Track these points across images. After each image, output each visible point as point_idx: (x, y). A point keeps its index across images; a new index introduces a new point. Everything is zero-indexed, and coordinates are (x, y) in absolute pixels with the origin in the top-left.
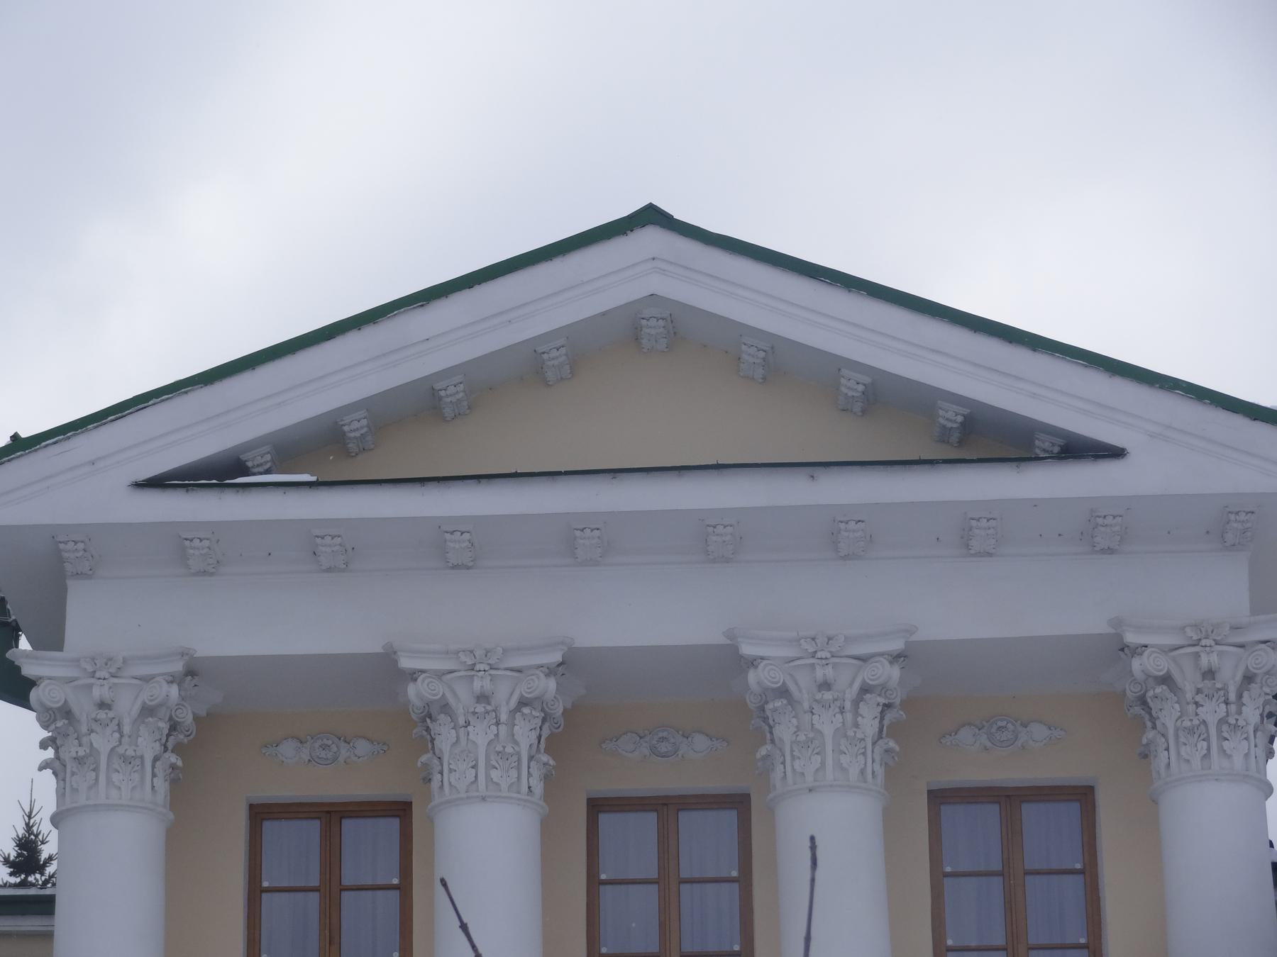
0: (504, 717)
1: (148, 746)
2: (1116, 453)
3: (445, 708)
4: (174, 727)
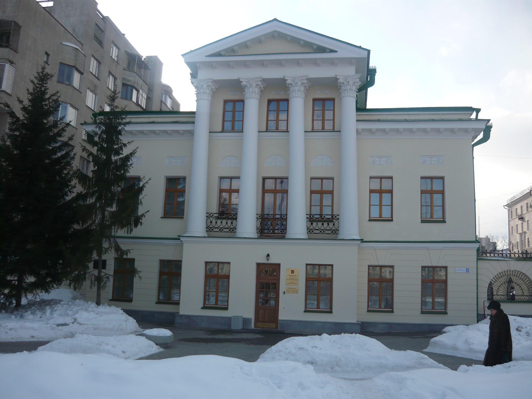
0: (254, 87)
1: (208, 91)
2: (336, 52)
3: (247, 86)
4: (212, 89)
